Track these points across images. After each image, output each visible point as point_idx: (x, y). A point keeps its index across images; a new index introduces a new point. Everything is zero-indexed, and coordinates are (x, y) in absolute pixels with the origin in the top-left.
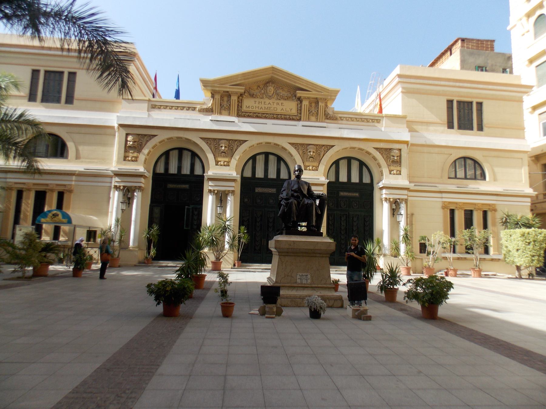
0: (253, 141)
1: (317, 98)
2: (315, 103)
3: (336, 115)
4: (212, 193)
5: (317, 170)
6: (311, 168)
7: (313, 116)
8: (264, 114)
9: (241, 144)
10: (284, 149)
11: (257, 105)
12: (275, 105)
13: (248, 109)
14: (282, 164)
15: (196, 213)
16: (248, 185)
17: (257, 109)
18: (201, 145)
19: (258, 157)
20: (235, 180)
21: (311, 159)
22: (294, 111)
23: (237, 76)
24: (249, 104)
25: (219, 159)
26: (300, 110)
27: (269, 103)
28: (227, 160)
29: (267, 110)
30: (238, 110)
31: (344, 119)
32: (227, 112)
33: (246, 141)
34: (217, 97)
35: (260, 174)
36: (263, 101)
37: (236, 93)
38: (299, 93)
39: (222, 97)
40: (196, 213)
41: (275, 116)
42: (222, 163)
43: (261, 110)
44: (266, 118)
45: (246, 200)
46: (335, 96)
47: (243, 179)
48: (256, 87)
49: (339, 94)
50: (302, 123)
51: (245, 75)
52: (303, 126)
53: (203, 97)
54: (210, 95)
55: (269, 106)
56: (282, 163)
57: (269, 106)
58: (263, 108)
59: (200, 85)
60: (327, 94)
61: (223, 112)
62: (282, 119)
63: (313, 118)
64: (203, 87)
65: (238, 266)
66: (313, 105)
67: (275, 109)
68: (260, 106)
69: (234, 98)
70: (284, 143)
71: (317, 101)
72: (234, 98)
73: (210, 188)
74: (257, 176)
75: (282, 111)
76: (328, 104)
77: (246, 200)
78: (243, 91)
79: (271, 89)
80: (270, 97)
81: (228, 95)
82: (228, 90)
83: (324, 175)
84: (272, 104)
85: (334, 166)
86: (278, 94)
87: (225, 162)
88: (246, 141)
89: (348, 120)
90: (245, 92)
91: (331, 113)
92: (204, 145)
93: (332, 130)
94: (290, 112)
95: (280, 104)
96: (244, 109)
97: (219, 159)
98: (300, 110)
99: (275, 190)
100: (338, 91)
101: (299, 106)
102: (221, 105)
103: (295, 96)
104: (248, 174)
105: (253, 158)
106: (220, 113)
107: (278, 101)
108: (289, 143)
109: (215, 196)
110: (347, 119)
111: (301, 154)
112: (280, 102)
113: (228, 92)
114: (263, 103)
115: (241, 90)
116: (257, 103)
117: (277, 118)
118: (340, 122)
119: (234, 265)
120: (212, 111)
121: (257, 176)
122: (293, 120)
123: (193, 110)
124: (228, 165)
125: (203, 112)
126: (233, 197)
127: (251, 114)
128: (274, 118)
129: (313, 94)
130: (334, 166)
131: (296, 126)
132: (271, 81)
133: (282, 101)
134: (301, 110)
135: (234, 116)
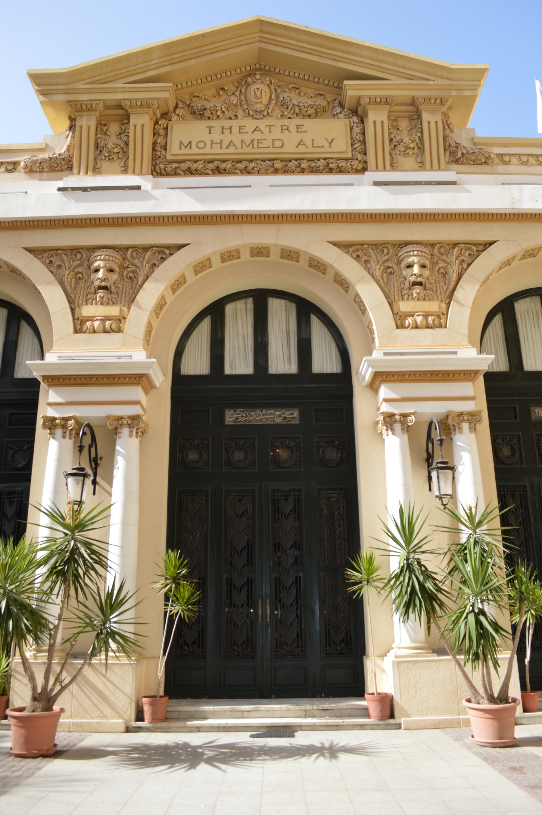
0: (207, 243)
1: (413, 102)
2: (411, 119)
3: (485, 148)
4: (59, 432)
5: (440, 326)
6: (419, 319)
7: (406, 155)
8: (240, 161)
9: (163, 259)
10: (318, 266)
11: (216, 136)
12: (276, 133)
13: (187, 151)
14: (316, 323)
15: (10, 511)
16: (196, 403)
17: (216, 149)
18: (26, 272)
19: (229, 308)
20: (141, 376)
21: (417, 289)
22: (342, 146)
23: (147, 53)
24: (188, 136)
25: (87, 311)
26: (360, 143)
27: (257, 129)
28: (114, 311)
29: (250, 150)
30: (155, 158)
31: (514, 160)
32: (117, 165)
33: (180, 247)
34: (88, 123)
35: (239, 361)
36: (235, 124)
37: (146, 105)
38: (353, 90)
39: (102, 126)
40: (10, 511)
41: (278, 165)
42: (96, 324)
43: (231, 150)
44: (246, 171)
45: (192, 456)
46: (475, 88)
47: (182, 385)
48: (213, 91)
49: (486, 83)
50: (370, 176)
51: (172, 50)
52: (376, 183)
53: (40, 128)
54: (67, 123)
55: (257, 135)
56: (315, 322)
57: (257, 135)
58: (239, 145)
59: (29, 90)
60: (446, 82)
61: (105, 165)
62: (303, 171)
63: (410, 162)
64: (42, 98)
65: (155, 719)
66: (404, 124)
67: (278, 144)
68: (227, 138)
69: (141, 122)
70: (314, 243)
71: (414, 112)
72: (141, 122)
73: (51, 412)
74: (228, 371)
75: (302, 149)
76: (454, 119)
77: (192, 456)
78: (166, 95)
79: (260, 91)
80: (260, 114)
81: (122, 114)
82: (119, 96)
83: (471, 343)
84: (266, 130)
85: (498, 320)
86: (283, 104)
87: (104, 319)
88: (180, 247)
89: (526, 163)
90: (176, 107)
91: (465, 143)
92: (35, 270)
93: (480, 193)
94: (327, 149)
95: (293, 128)
96: (174, 150)
97: (87, 311)
98: (360, 143)
99: (296, 414)
100: (483, 72)
101: (357, 130)
102: (97, 146)
103: (341, 105)
104: (197, 363)
105: (215, 312)
106: (96, 171)
107: (286, 122)
108: (335, 244)
109: (69, 443)
110: (524, 160)
111: (378, 274)
112: (293, 123)
113: (119, 106)
114: (235, 130)
115: (163, 93)
116: (216, 131)
117: (286, 171)
118: (501, 168)
119: (140, 717)
120: (70, 168)
121: (228, 371)
122: (341, 171)
123: (8, 171)
124: (119, 330)
125: (42, 171)
126: (135, 442)
127: (200, 165)
128: (276, 171)
129: (398, 89)
130: (498, 320)
131: (352, 185)
132: (262, 67)
133: (298, 121)
134: (364, 142)
135: (141, 174)
